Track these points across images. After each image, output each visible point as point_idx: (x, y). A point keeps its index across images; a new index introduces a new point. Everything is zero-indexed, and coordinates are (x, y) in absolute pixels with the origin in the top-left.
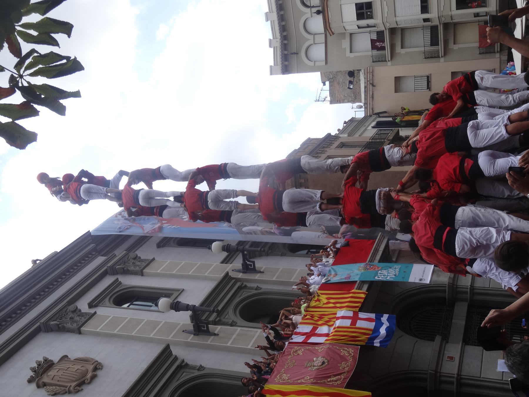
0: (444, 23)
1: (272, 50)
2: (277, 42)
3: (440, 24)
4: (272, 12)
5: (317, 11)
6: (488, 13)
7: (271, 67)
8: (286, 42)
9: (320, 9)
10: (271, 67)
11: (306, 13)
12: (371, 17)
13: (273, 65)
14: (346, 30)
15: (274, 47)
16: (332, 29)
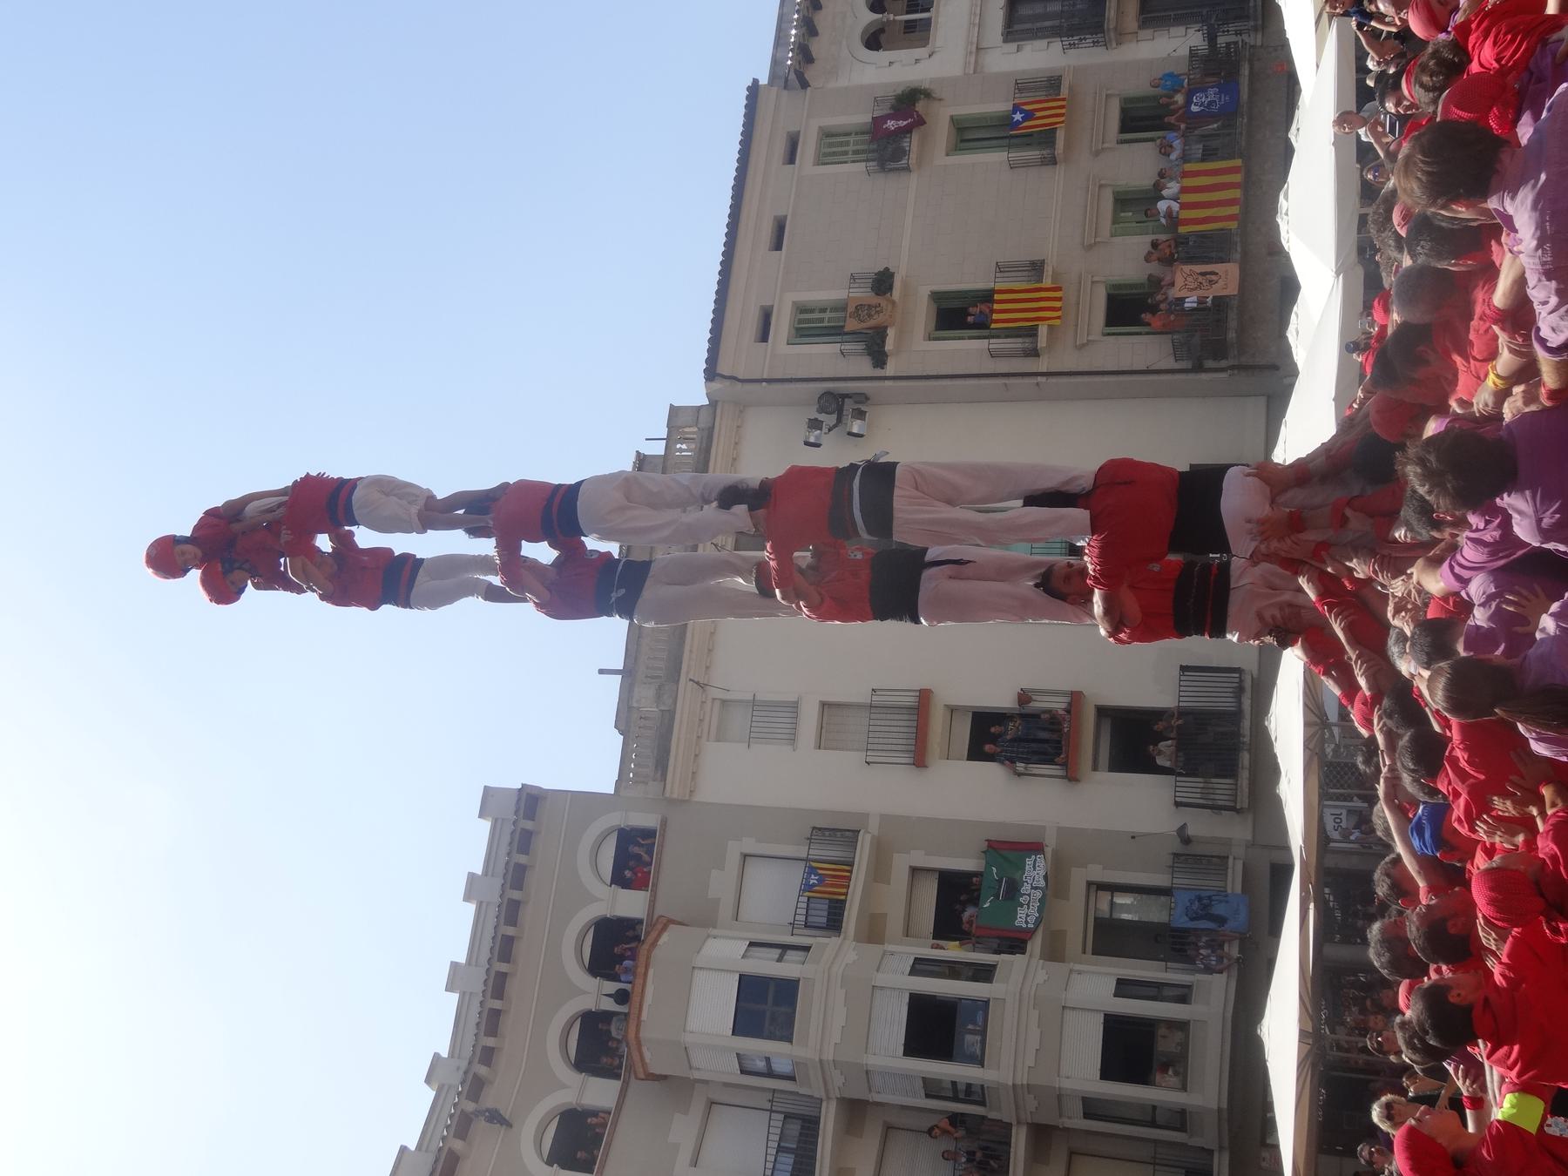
0: (1032, 1123)
1: (429, 1095)
2: (458, 1069)
3: (1019, 1123)
4: (476, 966)
5: (617, 991)
6: (1190, 1112)
7: (403, 1150)
8: (483, 1070)
10: (403, 1150)
11: (585, 993)
12: (784, 1030)
13: (412, 1146)
14: (691, 1068)
15: (443, 1085)
16: (644, 1049)
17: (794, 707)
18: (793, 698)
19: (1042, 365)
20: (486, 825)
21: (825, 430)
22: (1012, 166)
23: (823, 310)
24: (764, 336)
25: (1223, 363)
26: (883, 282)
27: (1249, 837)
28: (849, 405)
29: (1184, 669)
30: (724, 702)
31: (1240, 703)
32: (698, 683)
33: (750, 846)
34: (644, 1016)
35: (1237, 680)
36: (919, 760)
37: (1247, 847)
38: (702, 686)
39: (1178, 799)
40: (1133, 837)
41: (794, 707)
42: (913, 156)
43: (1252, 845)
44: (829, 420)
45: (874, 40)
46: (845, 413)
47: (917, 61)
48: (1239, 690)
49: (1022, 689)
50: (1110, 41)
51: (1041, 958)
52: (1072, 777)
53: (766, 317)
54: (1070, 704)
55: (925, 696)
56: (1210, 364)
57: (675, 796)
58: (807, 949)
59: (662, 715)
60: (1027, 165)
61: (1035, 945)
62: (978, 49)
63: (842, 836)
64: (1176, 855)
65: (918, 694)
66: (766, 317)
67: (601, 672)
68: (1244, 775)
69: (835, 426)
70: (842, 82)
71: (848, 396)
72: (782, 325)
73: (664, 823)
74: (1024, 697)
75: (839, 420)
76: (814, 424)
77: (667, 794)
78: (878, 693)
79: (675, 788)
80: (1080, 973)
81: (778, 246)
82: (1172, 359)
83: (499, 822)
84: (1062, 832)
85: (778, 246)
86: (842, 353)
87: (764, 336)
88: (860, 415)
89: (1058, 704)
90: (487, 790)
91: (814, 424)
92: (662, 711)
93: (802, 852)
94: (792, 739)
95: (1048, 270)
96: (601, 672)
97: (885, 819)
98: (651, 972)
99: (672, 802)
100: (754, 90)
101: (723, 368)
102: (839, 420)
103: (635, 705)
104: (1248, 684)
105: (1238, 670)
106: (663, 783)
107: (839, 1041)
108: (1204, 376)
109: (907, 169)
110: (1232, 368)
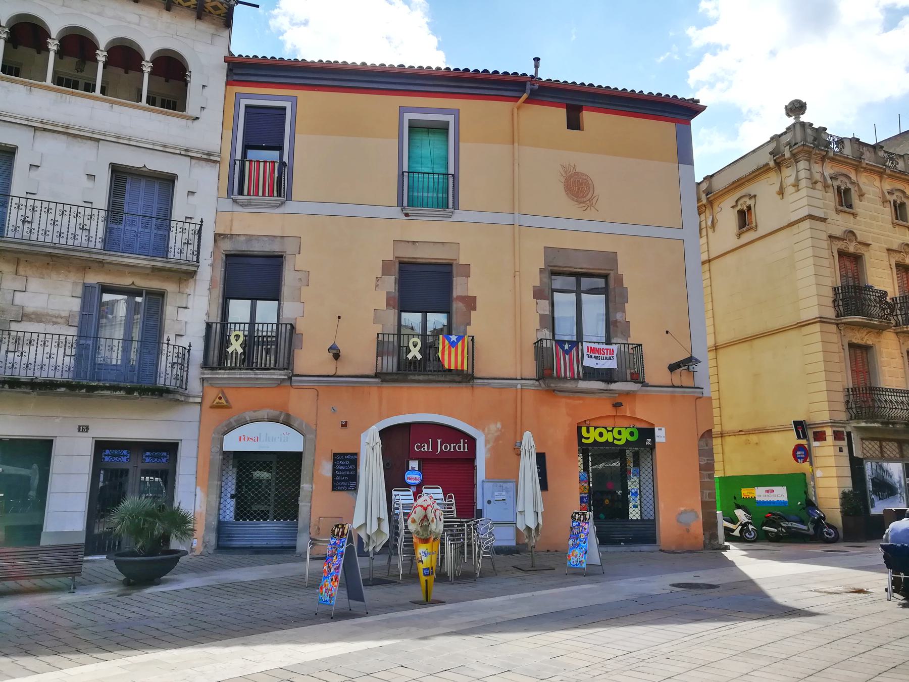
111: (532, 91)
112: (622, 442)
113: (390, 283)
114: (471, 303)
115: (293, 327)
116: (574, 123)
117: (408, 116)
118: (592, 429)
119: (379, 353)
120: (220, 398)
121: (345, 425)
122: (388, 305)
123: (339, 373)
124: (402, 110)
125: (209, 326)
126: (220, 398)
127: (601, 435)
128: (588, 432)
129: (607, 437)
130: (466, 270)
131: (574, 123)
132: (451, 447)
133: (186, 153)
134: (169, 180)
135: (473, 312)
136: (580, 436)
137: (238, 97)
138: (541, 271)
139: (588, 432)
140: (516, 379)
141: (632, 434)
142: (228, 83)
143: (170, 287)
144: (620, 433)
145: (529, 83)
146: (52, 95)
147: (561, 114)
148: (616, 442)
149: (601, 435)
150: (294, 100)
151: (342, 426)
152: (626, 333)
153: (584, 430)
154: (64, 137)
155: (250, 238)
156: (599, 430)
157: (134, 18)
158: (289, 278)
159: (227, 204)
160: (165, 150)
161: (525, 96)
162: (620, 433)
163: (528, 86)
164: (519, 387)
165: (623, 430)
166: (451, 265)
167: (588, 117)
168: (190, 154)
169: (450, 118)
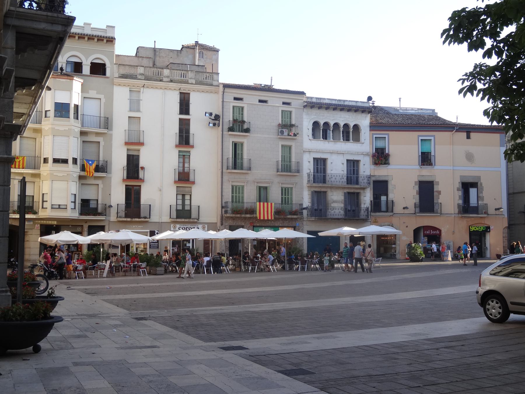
9: (64, 72)
17: (138, 111)
18: (141, 110)
19: (224, 170)
20: (105, 28)
21: (210, 117)
22: (277, 162)
23: (242, 114)
24: (235, 99)
25: (223, 213)
26: (247, 131)
27: (111, 220)
28: (217, 122)
29: (150, 205)
30: (140, 91)
31: (142, 218)
32: (144, 86)
33: (103, 100)
34: (57, 79)
35: (147, 217)
36: (126, 144)
37: (109, 220)
38: (144, 86)
39: (119, 205)
40: (110, 194)
41: (138, 111)
42: (281, 137)
43: (109, 221)
44: (213, 117)
45: (316, 124)
46: (215, 121)
47: (308, 136)
48: (145, 218)
49: (144, 168)
50: (308, 184)
51: (79, 175)
52: (124, 180)
53: (240, 99)
54: (141, 179)
55: (142, 144)
56: (224, 210)
57: (114, 81)
58: (77, 119)
59: (136, 75)
60: (278, 165)
61: (83, 173)
62: (310, 151)
63: (106, 125)
64: (106, 205)
65: (143, 142)
66: (240, 99)
67: (155, 42)
68: (125, 219)
69: (211, 119)
70: (305, 116)
71: (219, 121)
72: (238, 104)
73: (108, 78)
74: (143, 168)
75: (213, 120)
76: (211, 114)
77: (115, 79)
78: (143, 132)
79: (117, 81)
80: (76, 184)
81: (260, 101)
82: (224, 201)
83: (106, 31)
84: (111, 178)
85: (260, 101)
86: (230, 120)
87: (235, 99)
88: (214, 125)
89: (141, 175)
90: (114, 27)
91: (211, 114)
92: (137, 75)
93: (102, 115)
94: (131, 110)
95: (249, 172)
96: (155, 42)
97: (111, 135)
98: (69, 80)
99: (113, 80)
100: (303, 93)
101: (227, 90)
102: (213, 120)
103: (138, 68)
104: (146, 220)
105: (150, 218)
106: (118, 77)
107: (56, 129)
108: (220, 209)
109: (278, 135)
110: (222, 215)
111: (457, 129)
112: (481, 230)
113: (417, 187)
114: (439, 193)
115: (393, 201)
116: (468, 137)
117: (420, 138)
118: (473, 227)
119: (415, 207)
120: (376, 220)
121: (407, 227)
122: (417, 194)
123: (405, 213)
124: (419, 136)
125: (371, 201)
126: (376, 220)
127: (475, 228)
128: (472, 228)
129: (477, 229)
130: (438, 183)
131: (468, 137)
132: (435, 232)
133: (362, 154)
134: (358, 161)
135: (440, 195)
136: (470, 229)
137: (373, 134)
138: (459, 183)
139: (472, 228)
140: (452, 214)
141: (484, 228)
142: (370, 131)
143: (362, 191)
144: (480, 228)
145: (456, 127)
146: (333, 143)
147: (465, 134)
148: (479, 230)
149: (475, 228)
150: (388, 135)
151: (406, 227)
152: (483, 199)
153: (471, 227)
154: (336, 154)
155: (379, 176)
156: (475, 227)
157: (347, 117)
158: (390, 187)
159: (373, 167)
160: (358, 154)
161: (455, 131)
162: (480, 228)
163: (456, 128)
164: (453, 216)
165: (481, 227)
166: (433, 182)
167: (472, 135)
168: (363, 154)
169: (432, 138)
